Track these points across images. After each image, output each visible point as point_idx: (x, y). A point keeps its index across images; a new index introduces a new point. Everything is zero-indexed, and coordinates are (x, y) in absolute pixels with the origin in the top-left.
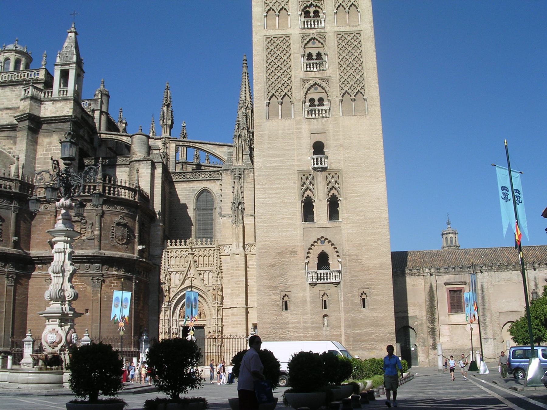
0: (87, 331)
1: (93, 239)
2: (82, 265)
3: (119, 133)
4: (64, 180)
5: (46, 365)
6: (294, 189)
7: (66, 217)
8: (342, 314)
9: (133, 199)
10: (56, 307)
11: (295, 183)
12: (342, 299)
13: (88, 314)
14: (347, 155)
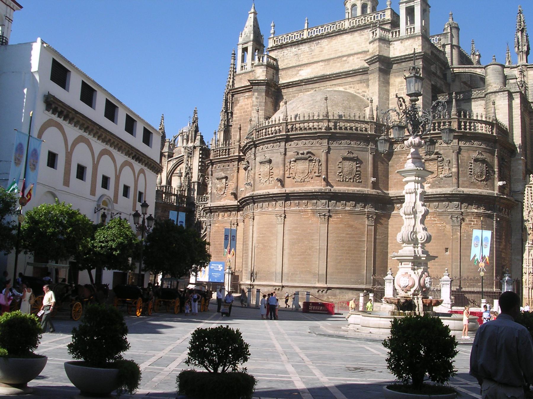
0: (447, 270)
1: (451, 177)
2: (440, 203)
3: (472, 66)
4: (411, 118)
5: (398, 310)
7: (416, 156)
9: (491, 133)
10: (408, 250)
13: (448, 253)
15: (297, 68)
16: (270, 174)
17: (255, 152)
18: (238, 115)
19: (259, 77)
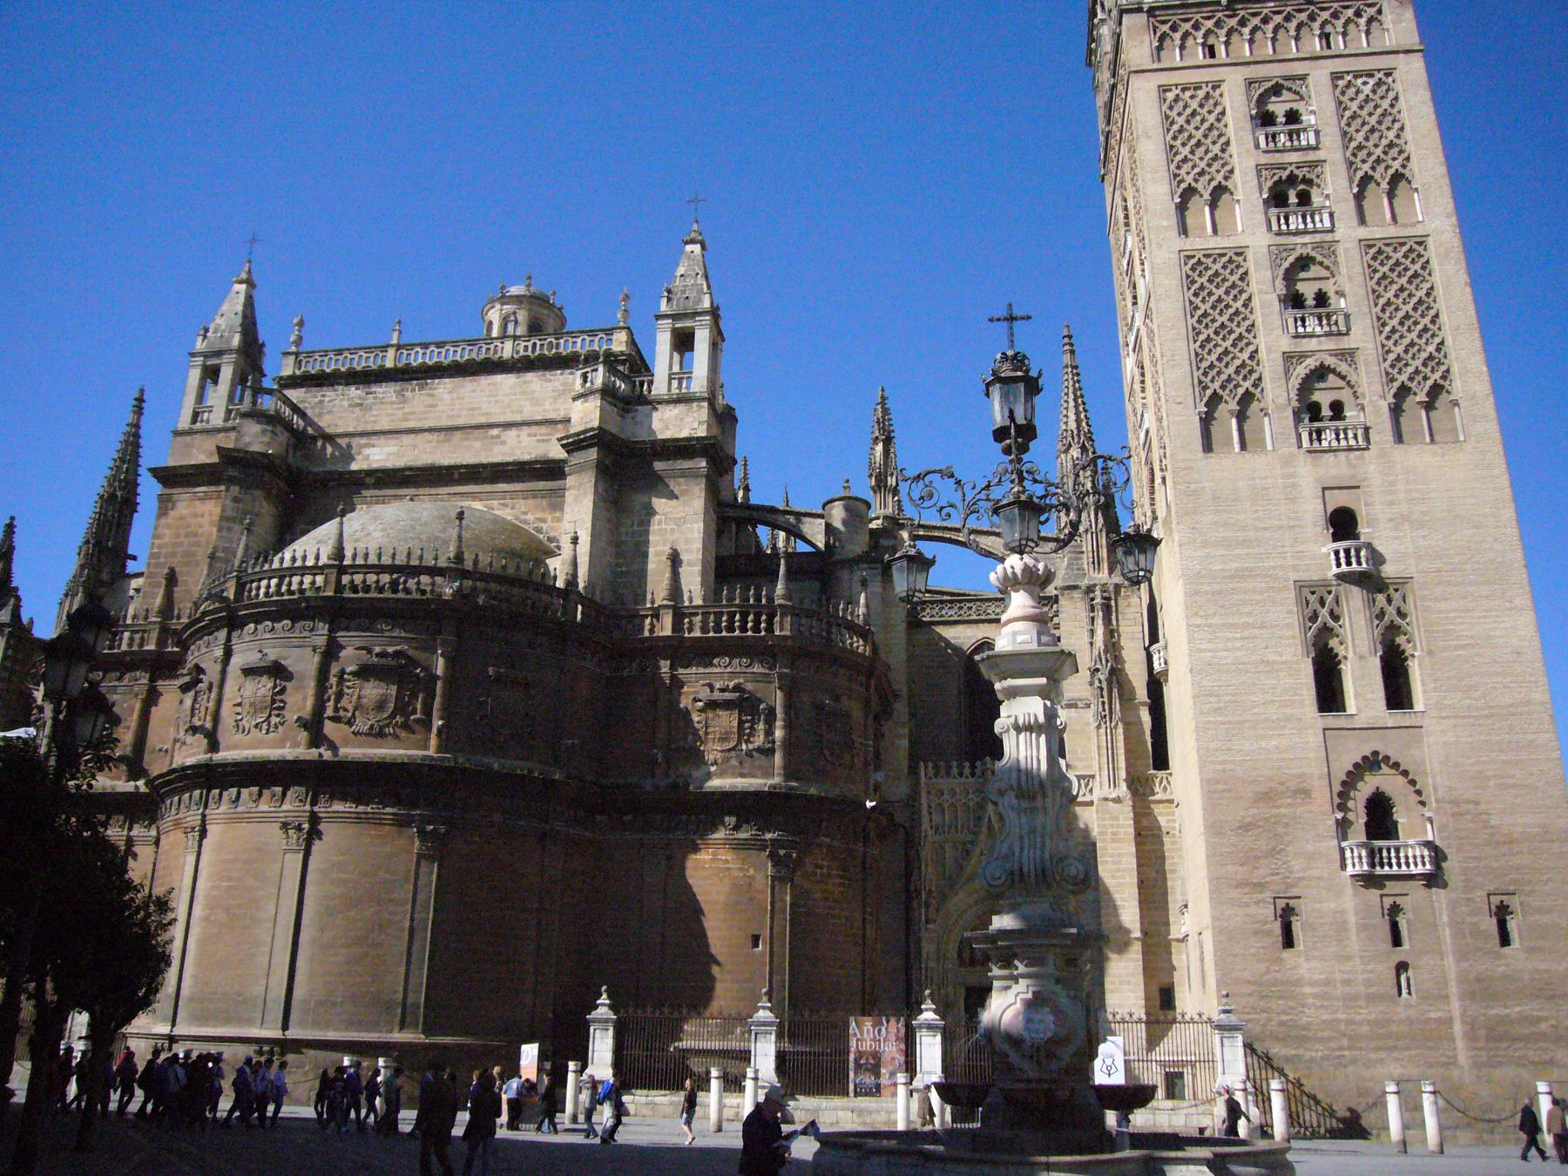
6: (1289, 626)
8: (1450, 962)
11: (1290, 612)
12: (1445, 918)
14: (1422, 542)
16: (276, 704)
17: (229, 639)
18: (166, 540)
19: (249, 444)
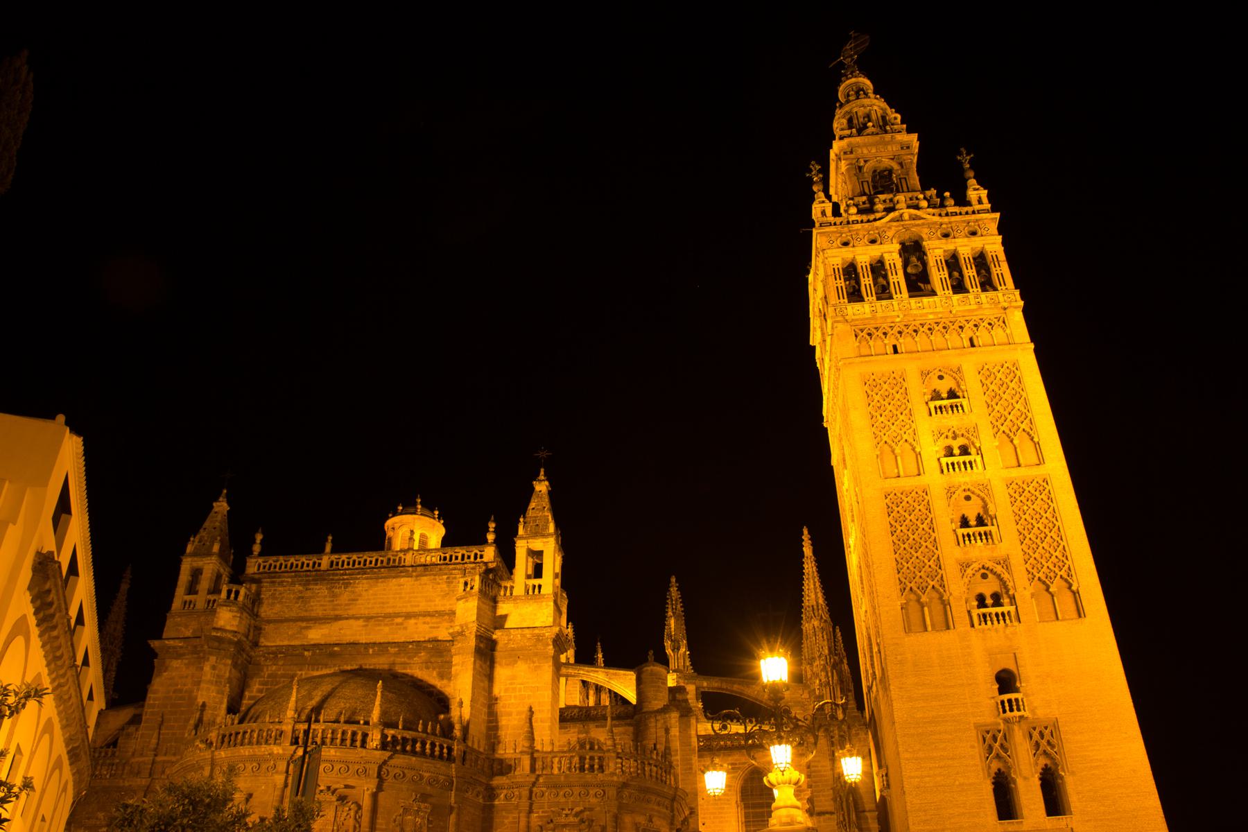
11: (973, 747)
15: (300, 624)
